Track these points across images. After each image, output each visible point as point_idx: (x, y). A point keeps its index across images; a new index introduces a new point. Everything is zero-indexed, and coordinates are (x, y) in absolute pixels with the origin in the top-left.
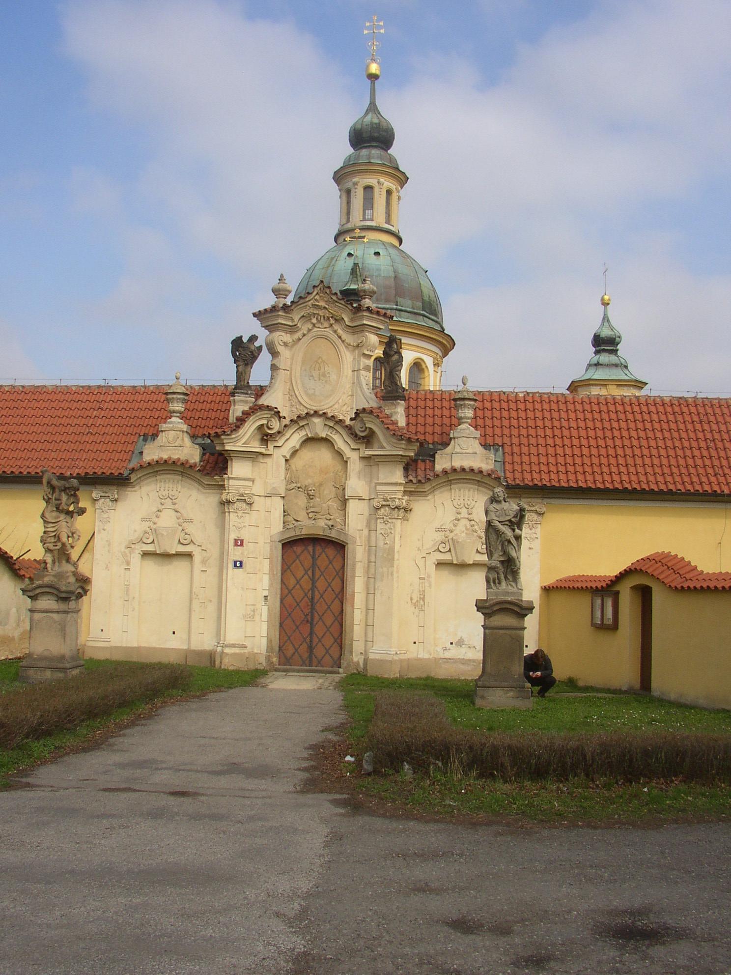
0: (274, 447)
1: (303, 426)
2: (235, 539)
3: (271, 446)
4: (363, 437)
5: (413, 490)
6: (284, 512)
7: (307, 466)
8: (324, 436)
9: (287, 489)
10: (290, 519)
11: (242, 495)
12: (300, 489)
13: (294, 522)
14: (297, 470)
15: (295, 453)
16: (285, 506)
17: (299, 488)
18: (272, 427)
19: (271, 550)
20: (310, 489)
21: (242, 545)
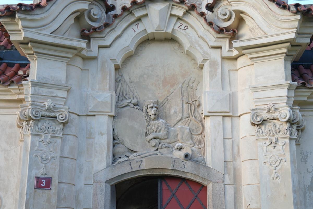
0: (100, 47)
1: (139, 19)
2: (38, 178)
3: (94, 44)
4: (227, 29)
5: (305, 99)
6: (114, 139)
7: (145, 76)
8: (170, 31)
9: (117, 107)
10: (120, 149)
11: (49, 110)
12: (136, 107)
13: (128, 154)
14: (131, 82)
15: (129, 58)
16: (115, 131)
17: (134, 105)
18: (95, 17)
19: (95, 195)
20: (152, 105)
21: (48, 186)
